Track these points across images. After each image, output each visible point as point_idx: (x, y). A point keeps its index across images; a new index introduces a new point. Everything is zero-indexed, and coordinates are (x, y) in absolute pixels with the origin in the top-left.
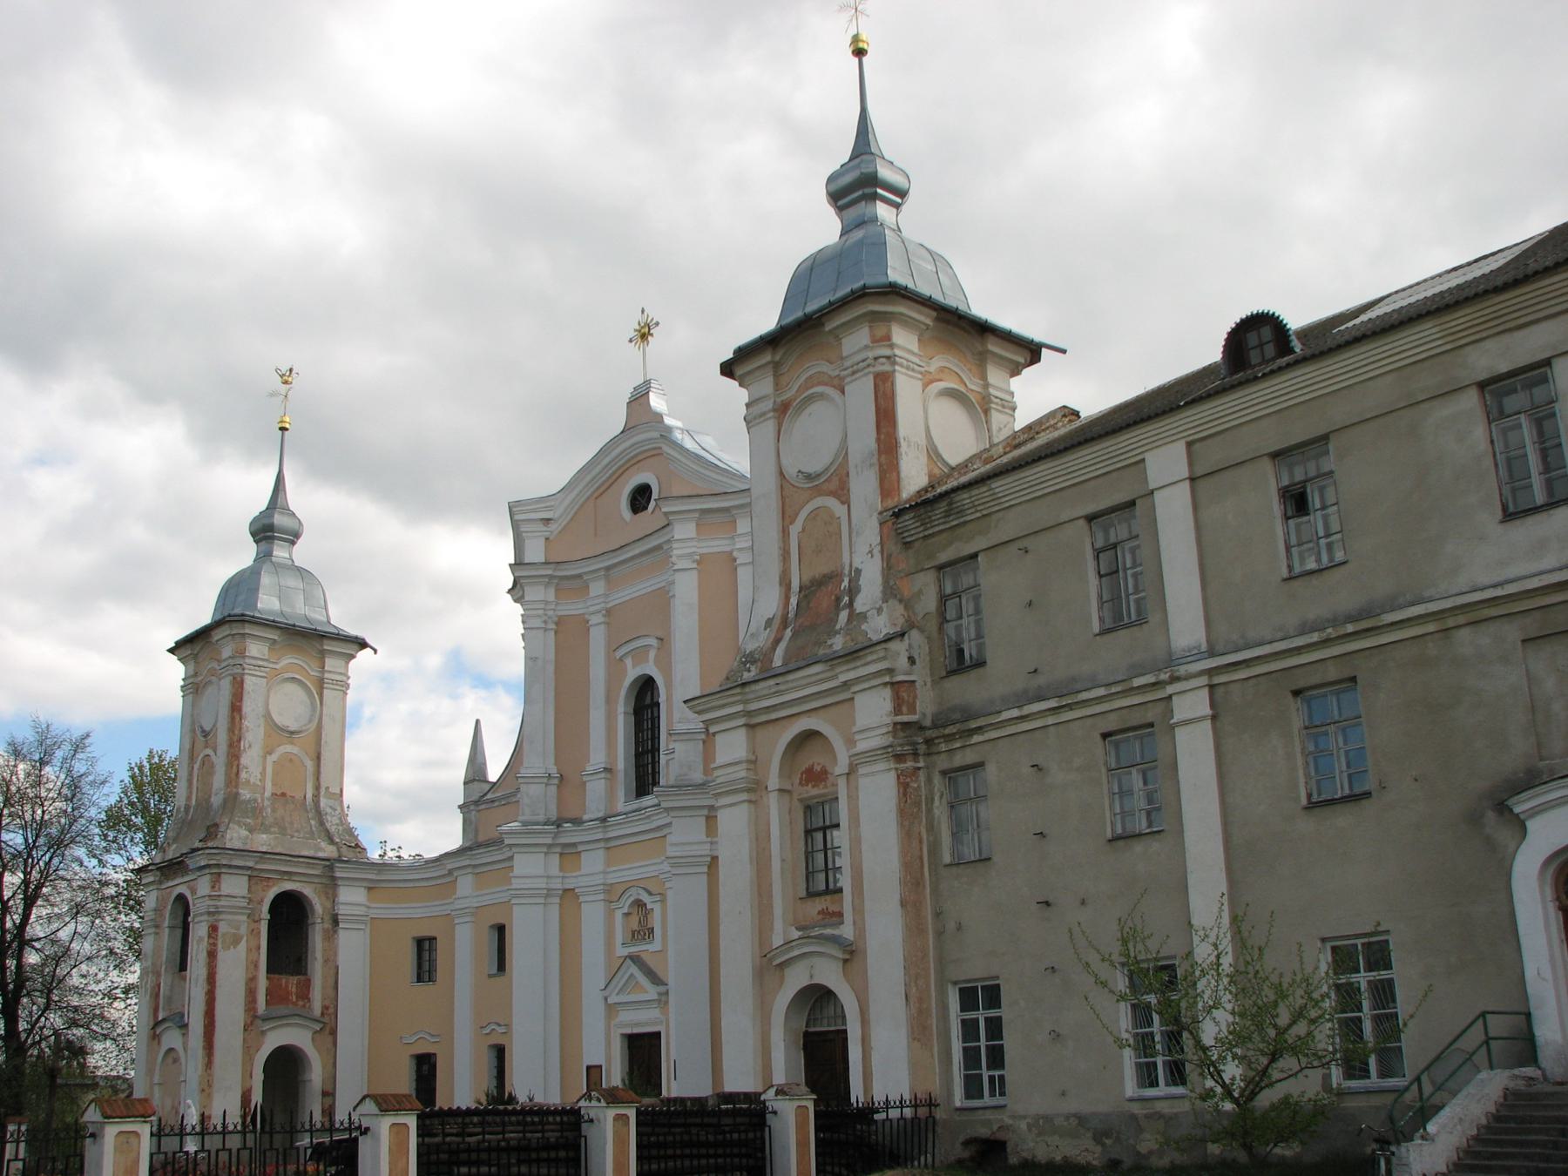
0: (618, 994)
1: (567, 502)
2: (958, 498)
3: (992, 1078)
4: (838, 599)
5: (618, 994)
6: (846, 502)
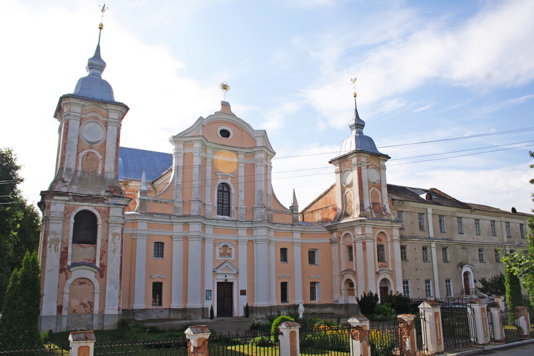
0: (220, 271)
4: (380, 208)
5: (220, 271)
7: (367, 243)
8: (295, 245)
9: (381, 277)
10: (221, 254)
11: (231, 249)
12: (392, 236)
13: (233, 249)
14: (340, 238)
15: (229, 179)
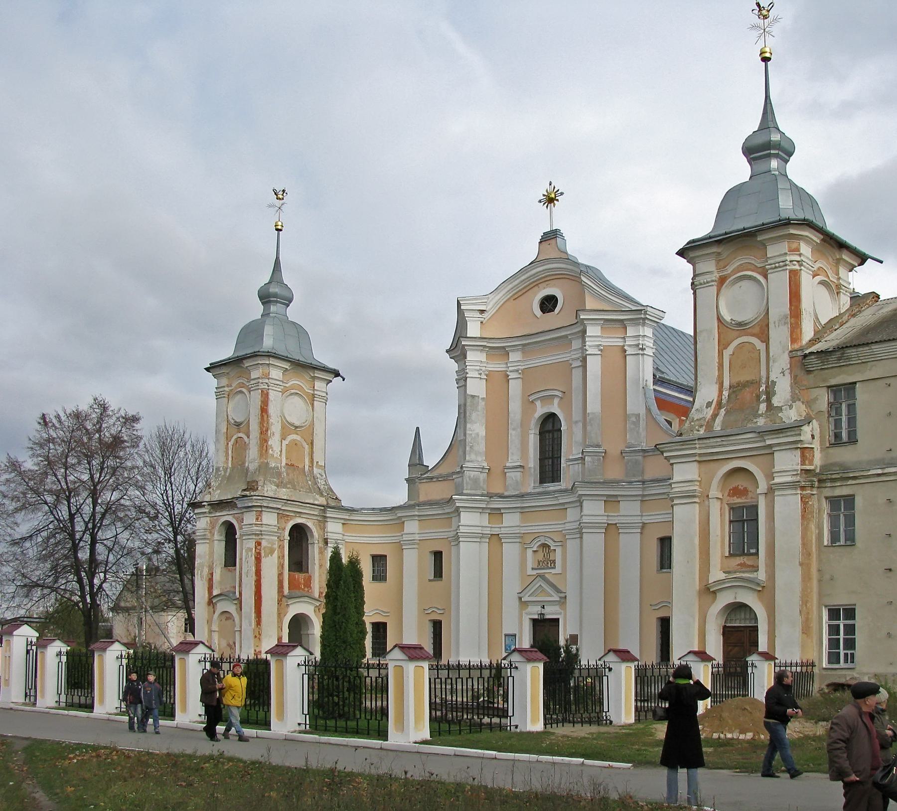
1: (494, 301)
2: (848, 351)
3: (846, 655)
6: (766, 340)
13: (559, 551)
15: (556, 401)
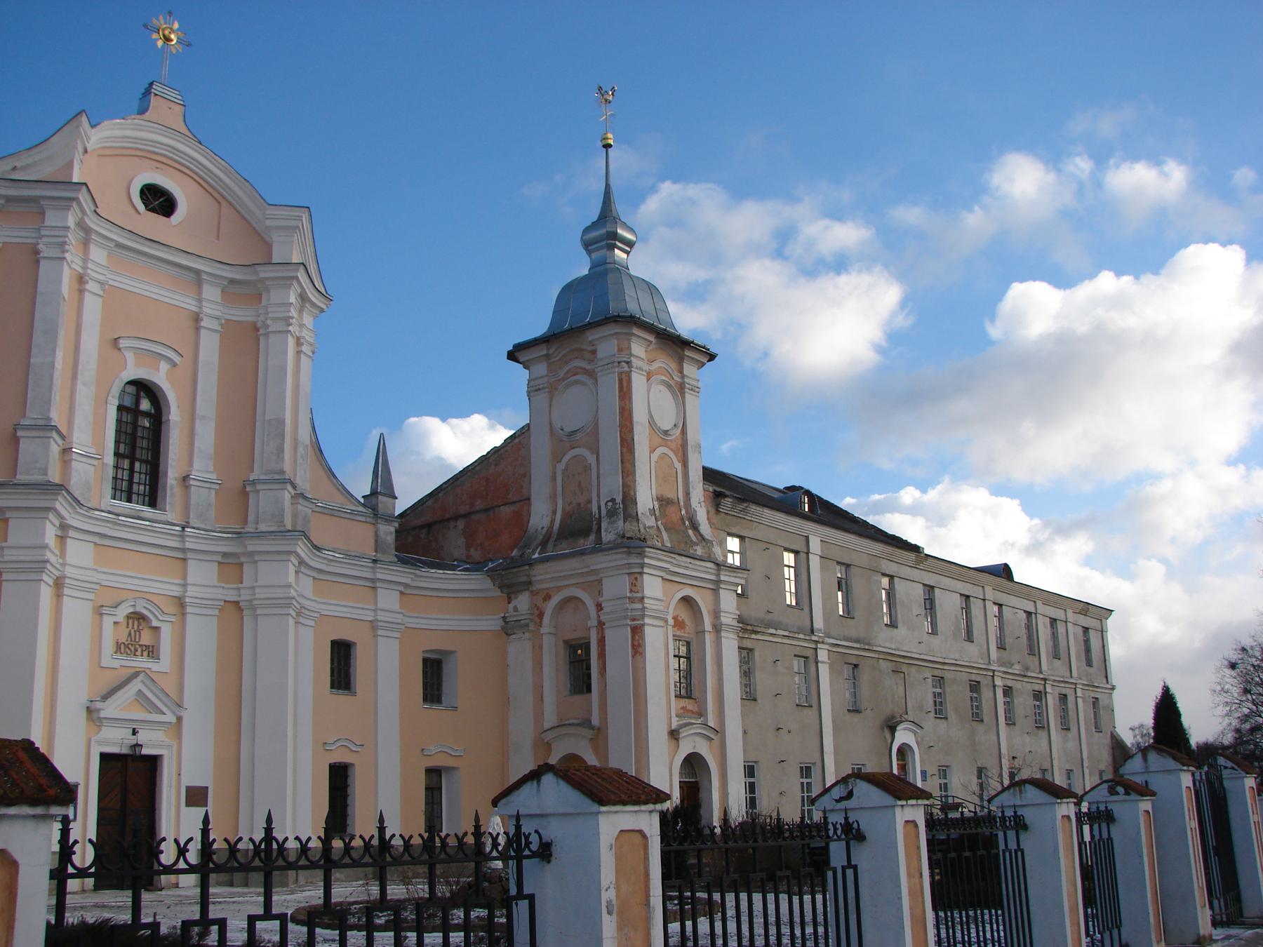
7: (647, 630)
8: (380, 632)
9: (686, 749)
10: (119, 647)
11: (157, 629)
12: (716, 614)
14: (541, 615)
